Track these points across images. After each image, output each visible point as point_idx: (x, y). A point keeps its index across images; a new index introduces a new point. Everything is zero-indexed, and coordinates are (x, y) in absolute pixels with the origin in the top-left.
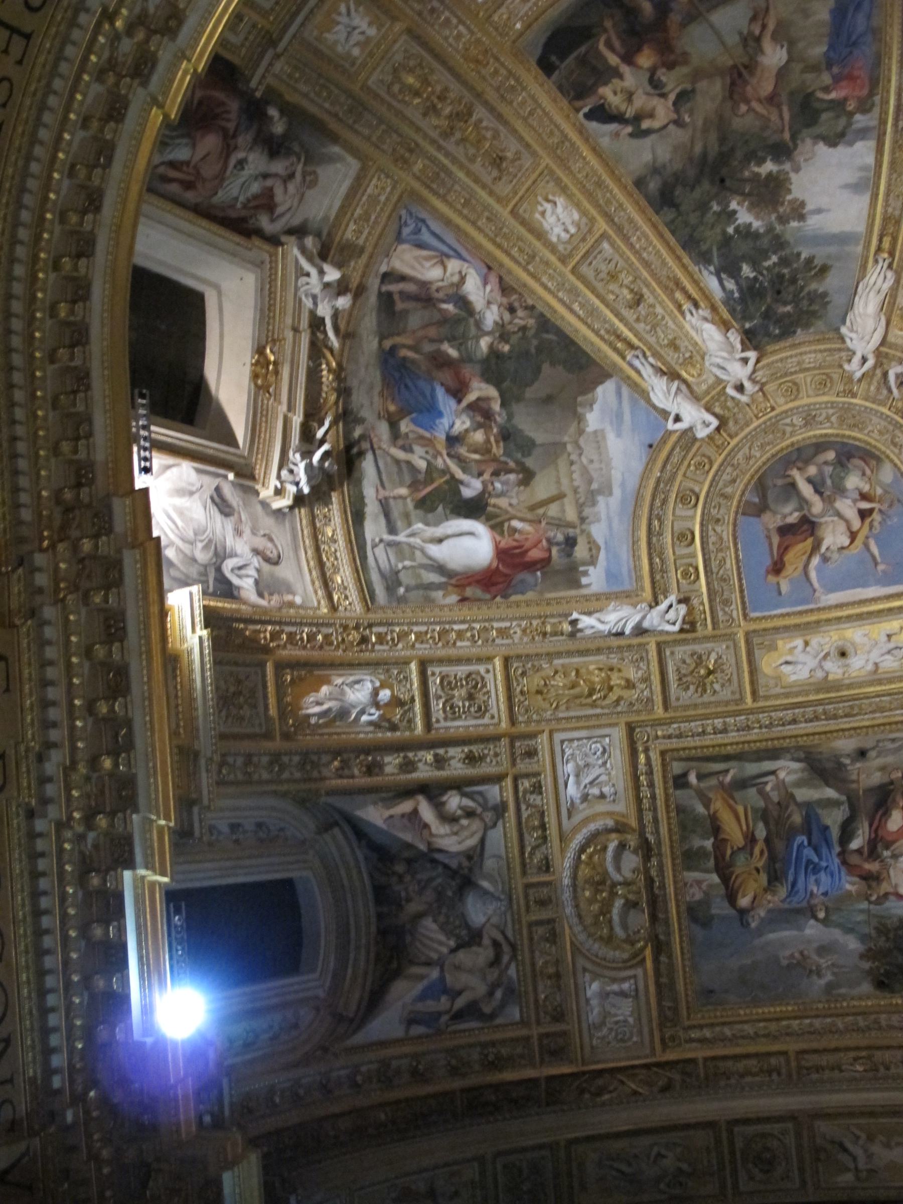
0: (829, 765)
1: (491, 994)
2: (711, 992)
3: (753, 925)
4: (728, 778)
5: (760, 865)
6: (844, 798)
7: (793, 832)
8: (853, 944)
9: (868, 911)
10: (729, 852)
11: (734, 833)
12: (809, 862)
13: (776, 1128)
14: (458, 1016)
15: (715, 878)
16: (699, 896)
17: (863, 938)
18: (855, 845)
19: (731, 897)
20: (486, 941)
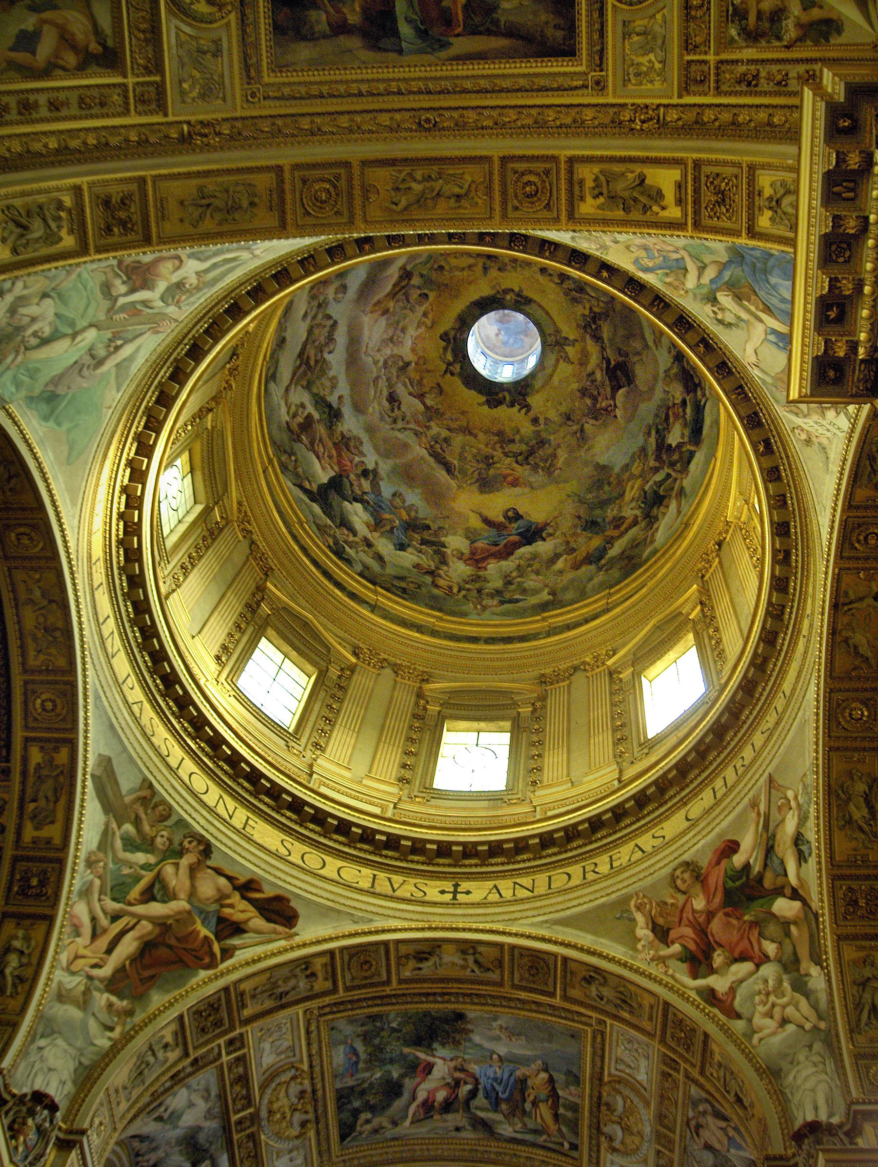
0: (480, 1127)
1: (704, 1113)
2: (572, 1036)
3: (540, 1062)
4: (544, 1137)
5: (531, 1090)
6: (472, 1110)
7: (508, 1100)
8: (477, 1038)
9: (465, 1053)
10: (550, 1102)
11: (545, 1110)
12: (500, 1084)
13: (524, 983)
14: (725, 1119)
15: (560, 1093)
16: (572, 1088)
17: (470, 1040)
18: (469, 1087)
19: (551, 1080)
20: (703, 1142)
